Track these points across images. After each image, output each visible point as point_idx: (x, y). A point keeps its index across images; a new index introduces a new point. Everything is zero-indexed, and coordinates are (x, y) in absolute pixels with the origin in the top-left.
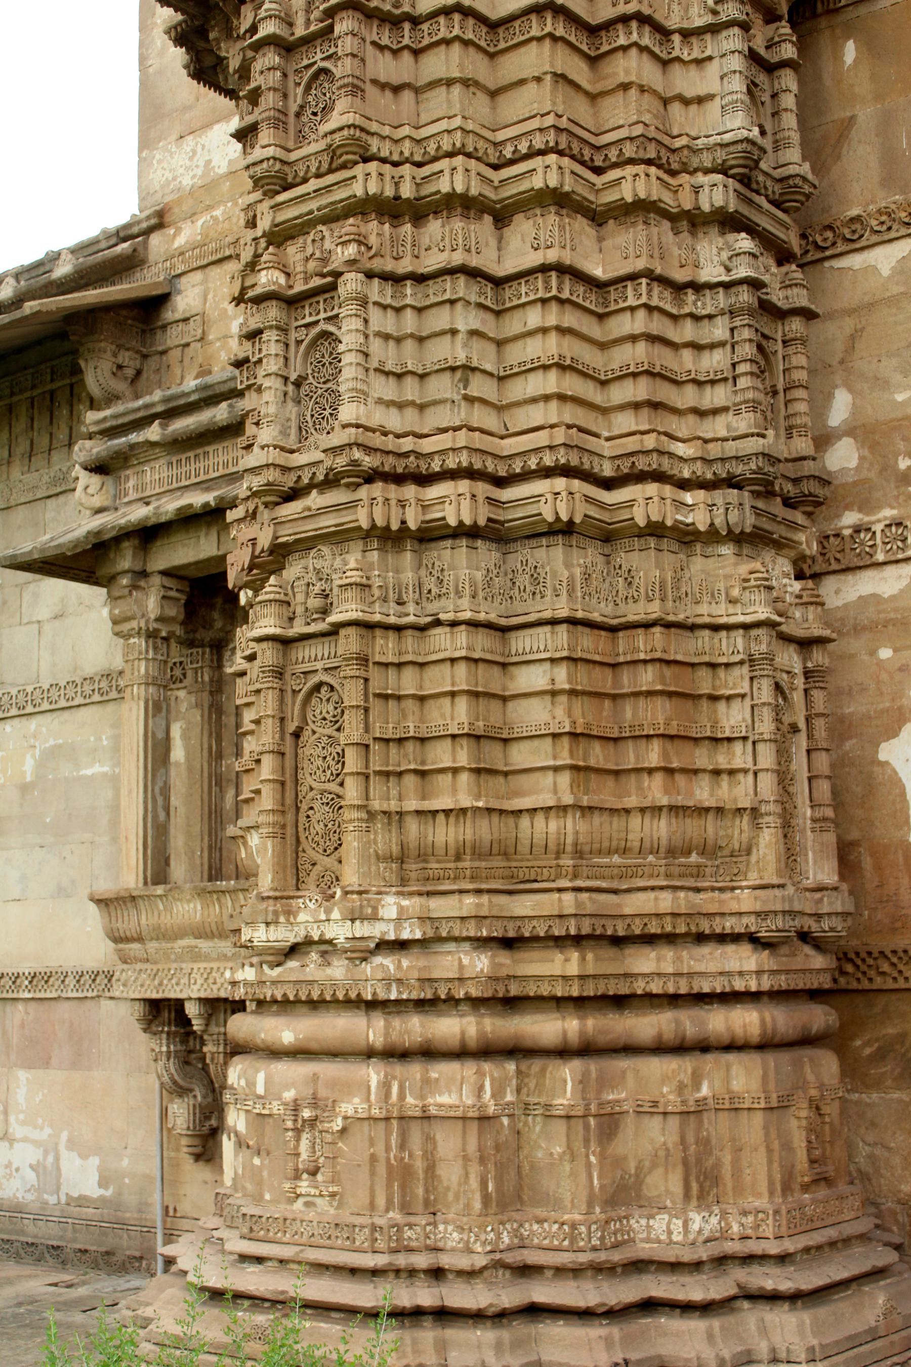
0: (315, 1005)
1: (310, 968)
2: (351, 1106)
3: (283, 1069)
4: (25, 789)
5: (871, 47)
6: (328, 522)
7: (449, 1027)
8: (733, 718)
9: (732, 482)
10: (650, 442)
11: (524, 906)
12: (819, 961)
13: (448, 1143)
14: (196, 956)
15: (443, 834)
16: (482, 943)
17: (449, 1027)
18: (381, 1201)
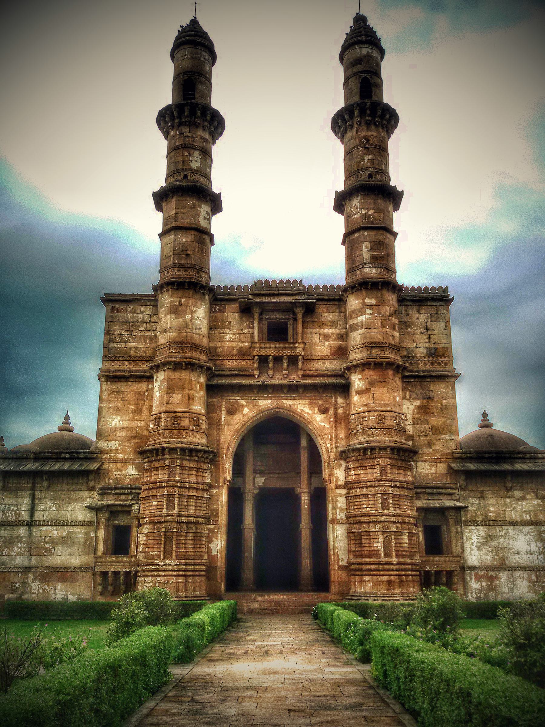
3: (162, 578)
4: (63, 537)
5: (215, 467)
6: (171, 520)
7: (181, 573)
8: (204, 542)
9: (205, 518)
14: (112, 565)
15: (181, 553)
16: (184, 565)
17: (181, 573)
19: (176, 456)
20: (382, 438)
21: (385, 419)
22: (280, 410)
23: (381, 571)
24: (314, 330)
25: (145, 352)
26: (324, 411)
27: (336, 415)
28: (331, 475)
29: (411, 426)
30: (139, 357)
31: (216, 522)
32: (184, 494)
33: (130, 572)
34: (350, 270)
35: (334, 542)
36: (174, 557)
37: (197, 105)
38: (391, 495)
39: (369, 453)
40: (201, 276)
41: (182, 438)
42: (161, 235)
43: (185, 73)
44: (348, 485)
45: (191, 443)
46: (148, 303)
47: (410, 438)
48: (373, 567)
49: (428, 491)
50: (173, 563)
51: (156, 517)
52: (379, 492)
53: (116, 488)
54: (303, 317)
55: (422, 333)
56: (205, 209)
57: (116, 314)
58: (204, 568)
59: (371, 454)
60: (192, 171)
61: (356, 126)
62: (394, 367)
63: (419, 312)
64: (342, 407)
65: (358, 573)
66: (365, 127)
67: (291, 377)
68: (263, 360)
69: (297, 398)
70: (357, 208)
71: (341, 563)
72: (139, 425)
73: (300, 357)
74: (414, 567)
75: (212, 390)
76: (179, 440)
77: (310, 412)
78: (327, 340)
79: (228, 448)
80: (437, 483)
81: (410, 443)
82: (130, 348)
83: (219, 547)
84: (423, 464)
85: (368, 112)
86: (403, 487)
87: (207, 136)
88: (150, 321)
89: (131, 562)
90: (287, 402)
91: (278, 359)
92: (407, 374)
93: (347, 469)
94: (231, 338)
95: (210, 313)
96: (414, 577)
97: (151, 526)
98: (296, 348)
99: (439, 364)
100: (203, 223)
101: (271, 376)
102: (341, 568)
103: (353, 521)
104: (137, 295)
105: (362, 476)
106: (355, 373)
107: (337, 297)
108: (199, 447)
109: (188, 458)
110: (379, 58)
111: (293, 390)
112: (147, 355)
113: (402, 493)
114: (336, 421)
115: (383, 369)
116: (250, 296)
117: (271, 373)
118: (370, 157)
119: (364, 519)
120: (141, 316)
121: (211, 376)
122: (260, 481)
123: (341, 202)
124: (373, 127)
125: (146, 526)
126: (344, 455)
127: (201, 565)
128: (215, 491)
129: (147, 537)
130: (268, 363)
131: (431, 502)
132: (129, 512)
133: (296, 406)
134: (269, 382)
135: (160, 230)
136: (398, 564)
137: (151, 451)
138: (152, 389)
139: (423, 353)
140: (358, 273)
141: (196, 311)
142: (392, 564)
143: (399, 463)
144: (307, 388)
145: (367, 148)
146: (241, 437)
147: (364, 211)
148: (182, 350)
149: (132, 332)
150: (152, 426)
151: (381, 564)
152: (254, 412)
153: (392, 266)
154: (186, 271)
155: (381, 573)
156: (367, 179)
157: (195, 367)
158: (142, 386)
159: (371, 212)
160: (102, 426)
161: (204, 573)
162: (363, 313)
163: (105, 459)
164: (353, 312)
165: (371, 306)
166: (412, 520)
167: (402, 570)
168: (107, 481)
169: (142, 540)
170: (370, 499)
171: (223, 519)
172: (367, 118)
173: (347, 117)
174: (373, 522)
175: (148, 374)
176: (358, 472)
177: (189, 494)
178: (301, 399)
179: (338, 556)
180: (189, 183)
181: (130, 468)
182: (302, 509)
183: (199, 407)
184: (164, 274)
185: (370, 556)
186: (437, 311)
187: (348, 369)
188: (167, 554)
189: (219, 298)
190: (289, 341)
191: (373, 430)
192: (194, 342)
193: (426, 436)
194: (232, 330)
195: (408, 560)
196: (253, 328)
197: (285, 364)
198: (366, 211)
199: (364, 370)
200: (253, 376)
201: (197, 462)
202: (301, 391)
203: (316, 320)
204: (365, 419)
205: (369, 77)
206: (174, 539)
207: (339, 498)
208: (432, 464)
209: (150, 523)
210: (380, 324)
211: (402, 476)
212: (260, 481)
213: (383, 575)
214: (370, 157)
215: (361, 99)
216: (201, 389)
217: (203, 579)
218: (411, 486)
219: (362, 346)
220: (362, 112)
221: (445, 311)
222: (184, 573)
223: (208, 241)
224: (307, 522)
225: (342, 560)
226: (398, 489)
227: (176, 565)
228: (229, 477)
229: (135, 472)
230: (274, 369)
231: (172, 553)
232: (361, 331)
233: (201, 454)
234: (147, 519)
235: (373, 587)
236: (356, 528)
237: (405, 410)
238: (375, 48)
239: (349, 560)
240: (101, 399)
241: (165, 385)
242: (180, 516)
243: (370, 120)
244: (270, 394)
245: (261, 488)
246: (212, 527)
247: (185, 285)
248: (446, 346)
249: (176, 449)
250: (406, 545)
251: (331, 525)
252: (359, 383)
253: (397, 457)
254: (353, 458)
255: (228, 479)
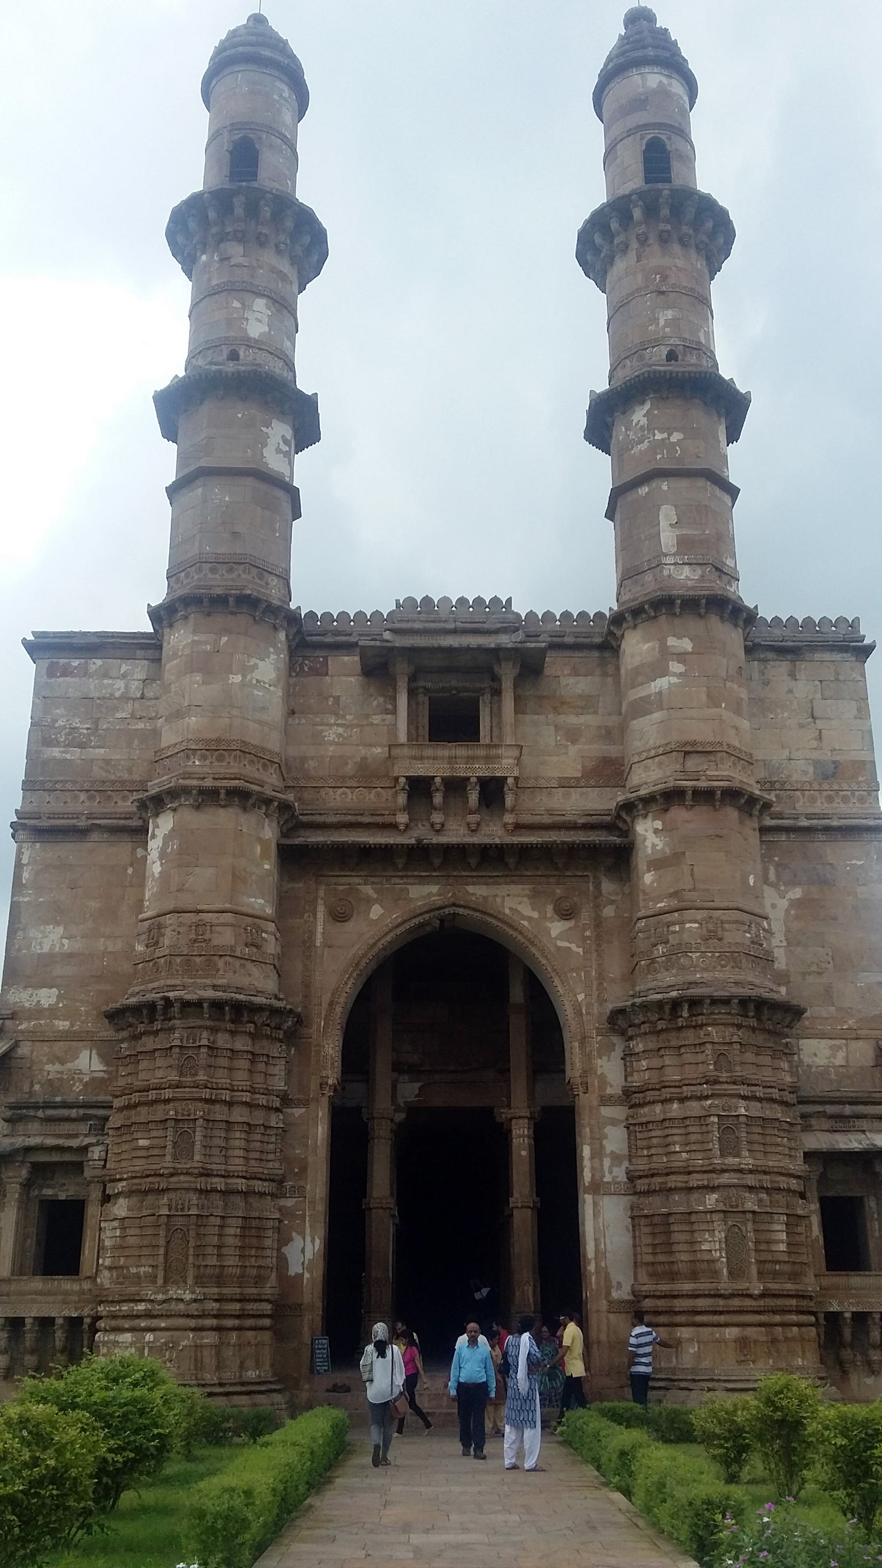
0: (168, 1316)
1: (173, 1306)
2: (184, 1343)
6: (186, 1185)
9: (273, 1180)
10: (261, 1170)
11: (225, 1291)
12: (269, 1307)
13: (206, 1353)
14: (34, 1301)
15: (209, 1271)
16: (216, 1300)
18: (192, 1367)
19: (199, 1022)
20: (717, 974)
21: (723, 929)
22: (461, 911)
23: (721, 1313)
24: (542, 718)
25: (130, 771)
26: (566, 914)
27: (598, 922)
28: (587, 1072)
29: (782, 951)
30: (114, 782)
31: (300, 1191)
32: (218, 1117)
33: (79, 1320)
34: (628, 575)
35: (596, 1240)
36: (190, 1281)
37: (262, 192)
38: (742, 1119)
39: (685, 1014)
40: (267, 584)
41: (214, 976)
42: (172, 491)
43: (234, 127)
44: (631, 1097)
45: (239, 990)
46: (139, 653)
47: (782, 978)
48: (702, 1303)
49: (830, 1109)
50: (188, 1296)
51: (148, 1176)
52: (714, 1111)
53: (47, 1106)
54: (515, 687)
55: (801, 726)
56: (279, 431)
57: (61, 679)
58: (267, 1308)
59: (691, 1015)
60: (250, 343)
61: (634, 245)
62: (743, 801)
63: (792, 675)
64: (612, 902)
65: (662, 1319)
66: (655, 248)
67: (485, 830)
68: (419, 788)
69: (501, 880)
70: (642, 428)
71: (615, 1295)
72: (110, 949)
73: (510, 781)
74: (804, 1303)
75: (295, 859)
76: (208, 981)
77: (535, 915)
78: (574, 742)
79: (331, 1004)
80: (848, 1089)
81: (783, 990)
82: (92, 760)
83: (309, 1255)
84: (814, 1042)
85: (665, 212)
86: (772, 1100)
87: (285, 266)
88: (142, 697)
89: (82, 1292)
90: (477, 891)
91: (455, 786)
92: (769, 822)
93: (628, 1056)
94: (339, 735)
95: (290, 676)
96: (803, 1329)
97: (135, 1199)
98: (499, 757)
99: (845, 799)
100: (274, 462)
101: (438, 827)
102: (617, 1307)
103: (637, 1185)
104: (113, 635)
105: (668, 1071)
106: (645, 816)
107: (598, 640)
108: (260, 1000)
109: (230, 1026)
110: (686, 99)
111: (493, 860)
112: (136, 777)
113: (768, 1114)
114: (599, 937)
115: (714, 806)
116: (387, 635)
117: (438, 820)
118: (670, 314)
119: (674, 1181)
120: (120, 684)
121: (290, 825)
122: (409, 1091)
123: (603, 422)
124: (676, 248)
125: (122, 1202)
126: (620, 1022)
127: (261, 1301)
128: (298, 1112)
129: (123, 1229)
130: (430, 797)
131: (837, 1136)
132: (78, 1167)
133: (498, 900)
134: (434, 841)
135: (171, 477)
136: (762, 1296)
137: (136, 1010)
138: (145, 858)
139: (805, 773)
140: (649, 577)
141: (256, 666)
142: (750, 1296)
143: (760, 1039)
144: (524, 853)
145: (663, 293)
146: (363, 979)
147: (659, 436)
148: (220, 759)
149: (96, 722)
150: (140, 948)
151: (720, 1296)
152: (396, 916)
153: (729, 562)
154: (231, 570)
155: (722, 1319)
156: (665, 362)
157: (251, 801)
158: (121, 850)
159: (676, 437)
160: (19, 950)
161: (267, 1322)
162: (665, 673)
163: (22, 1032)
164: (637, 671)
165: (681, 657)
166: (794, 1183)
167: (774, 1312)
168: (26, 1089)
169: (110, 1235)
170: (691, 1129)
171: (317, 1185)
172: (662, 226)
173: (614, 225)
174: (699, 1187)
175: (136, 823)
176: (656, 1062)
177: (232, 1120)
178: (513, 882)
179: (607, 1274)
180: (243, 368)
181: (85, 1055)
182: (515, 1157)
183: (263, 901)
184: (178, 579)
185: (694, 1276)
186: (837, 674)
187: (628, 807)
188: (172, 1273)
189: (310, 643)
190: (482, 742)
191: (694, 956)
192: (247, 739)
193: (819, 973)
194: (344, 717)
195: (789, 1286)
196: (394, 712)
197: (473, 797)
198: (665, 435)
199: (666, 810)
200: (394, 826)
201: (253, 1036)
202: (511, 861)
203: (546, 694)
204: (672, 928)
205: (664, 137)
206: (192, 1233)
207: (609, 1130)
208: (837, 1042)
209: (130, 1194)
210: (704, 697)
211: (767, 1072)
212: (409, 1091)
213: (726, 1325)
214: (670, 314)
215: (647, 181)
216: (264, 855)
217: (267, 1336)
218: (791, 1098)
219: (661, 751)
220: (651, 211)
221: (856, 675)
222: (214, 1322)
223: (287, 508)
224: (526, 1191)
225: (619, 1286)
226: (759, 1105)
227: (195, 1301)
228: (333, 1076)
229: (98, 1066)
230: (444, 808)
231: (185, 1269)
232: (657, 716)
233: (261, 1018)
234: (124, 1183)
235: (698, 1356)
236: (655, 1205)
237: (768, 911)
238: (676, 76)
239: (637, 1288)
240: (18, 885)
241: (174, 845)
242: (207, 1174)
243: (668, 231)
244: (435, 870)
245: (411, 1110)
246: (289, 1203)
247: (228, 602)
248: (863, 756)
249: (198, 1004)
250: (782, 1247)
251: (588, 1198)
252: (657, 841)
253: (754, 1022)
254: (645, 1028)
255: (330, 1082)
